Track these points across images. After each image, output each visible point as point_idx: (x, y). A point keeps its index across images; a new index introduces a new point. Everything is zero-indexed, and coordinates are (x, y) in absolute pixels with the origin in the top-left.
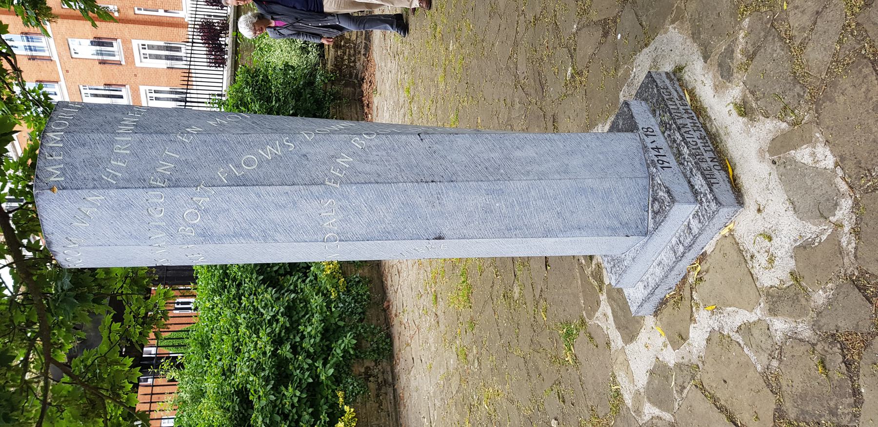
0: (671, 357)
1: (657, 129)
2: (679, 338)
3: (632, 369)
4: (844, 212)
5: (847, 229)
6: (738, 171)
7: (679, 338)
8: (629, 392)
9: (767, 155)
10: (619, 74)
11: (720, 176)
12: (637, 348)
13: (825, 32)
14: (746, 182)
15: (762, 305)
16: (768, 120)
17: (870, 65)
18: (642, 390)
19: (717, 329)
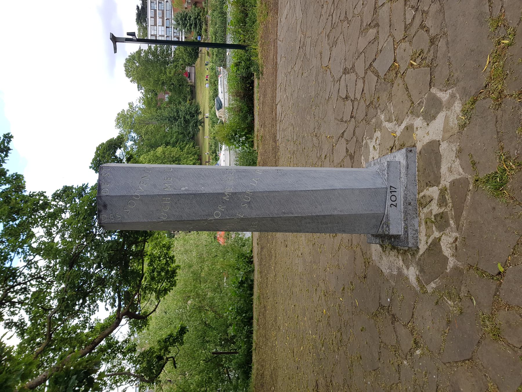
0: (418, 122)
2: (409, 128)
3: (443, 125)
7: (409, 128)
8: (453, 111)
12: (434, 136)
18: (444, 109)
19: (397, 125)
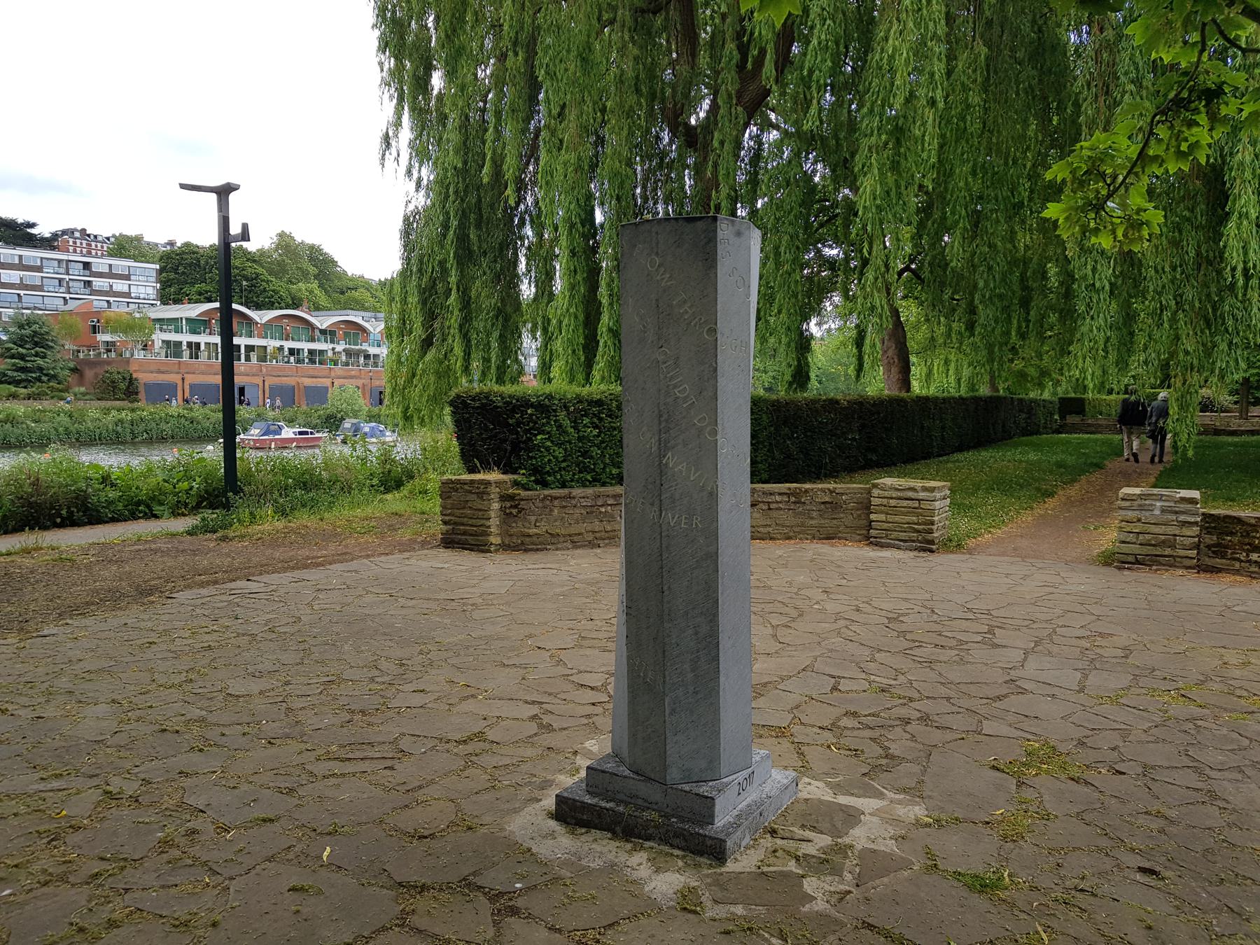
10: (569, 874)
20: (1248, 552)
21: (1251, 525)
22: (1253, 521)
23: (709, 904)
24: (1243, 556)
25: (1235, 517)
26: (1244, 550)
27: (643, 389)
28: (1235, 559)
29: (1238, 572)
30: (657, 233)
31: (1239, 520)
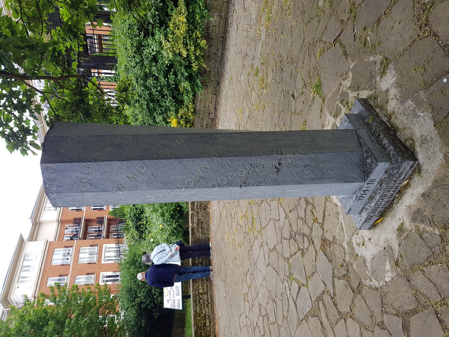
1: (376, 183)
4: (375, 283)
5: (371, 283)
6: (380, 225)
9: (386, 244)
11: (375, 218)
13: (427, 287)
14: (377, 230)
15: (348, 238)
16: (398, 246)
17: (415, 308)
20: (206, 327)
21: (197, 327)
22: (195, 327)
23: (378, 63)
24: (208, 328)
25: (195, 333)
26: (206, 328)
27: (150, 145)
28: (210, 331)
29: (214, 329)
30: (54, 137)
31: (196, 332)
